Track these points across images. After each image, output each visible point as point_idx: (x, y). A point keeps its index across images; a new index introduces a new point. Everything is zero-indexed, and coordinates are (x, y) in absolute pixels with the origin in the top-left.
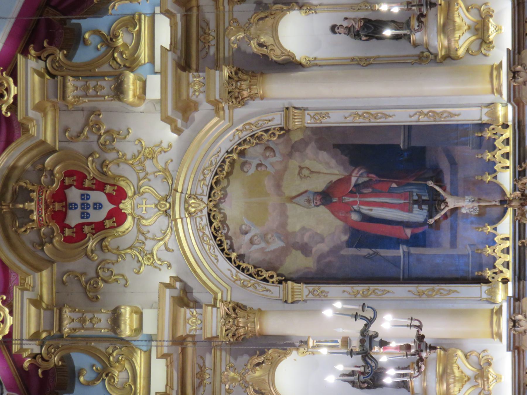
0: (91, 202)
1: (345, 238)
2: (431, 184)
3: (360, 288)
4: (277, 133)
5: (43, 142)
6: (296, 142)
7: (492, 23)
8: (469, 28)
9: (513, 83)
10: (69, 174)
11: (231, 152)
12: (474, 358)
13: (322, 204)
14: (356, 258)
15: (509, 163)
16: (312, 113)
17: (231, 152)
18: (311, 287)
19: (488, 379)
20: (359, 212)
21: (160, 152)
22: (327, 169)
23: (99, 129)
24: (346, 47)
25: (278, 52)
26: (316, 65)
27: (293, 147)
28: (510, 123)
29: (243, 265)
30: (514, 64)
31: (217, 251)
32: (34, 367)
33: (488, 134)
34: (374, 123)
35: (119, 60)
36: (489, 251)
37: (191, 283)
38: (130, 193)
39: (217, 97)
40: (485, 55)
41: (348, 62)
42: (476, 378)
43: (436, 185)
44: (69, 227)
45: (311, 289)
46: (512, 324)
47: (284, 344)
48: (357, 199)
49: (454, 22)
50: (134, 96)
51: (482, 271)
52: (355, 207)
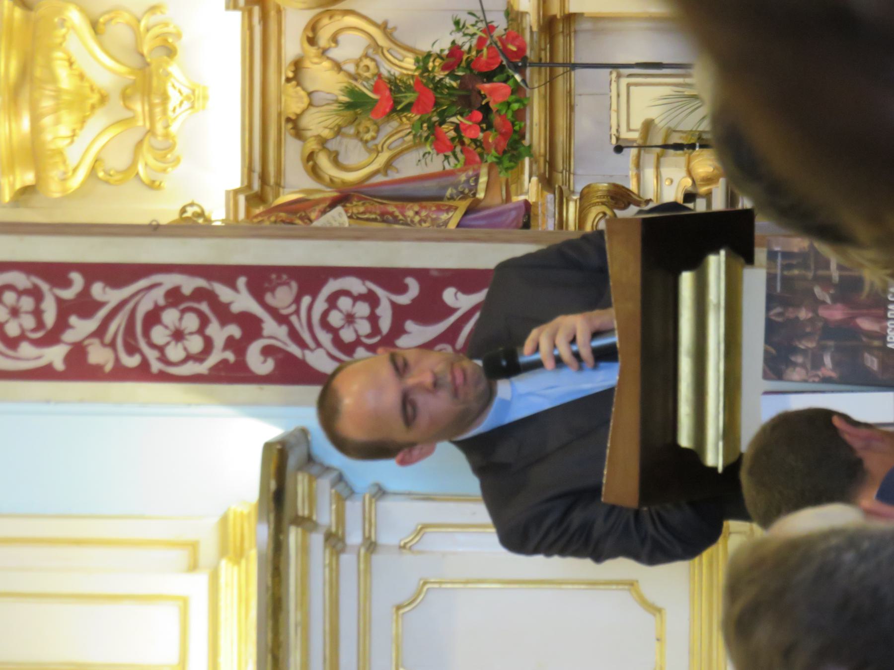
12: (119, 31)
19: (165, 98)
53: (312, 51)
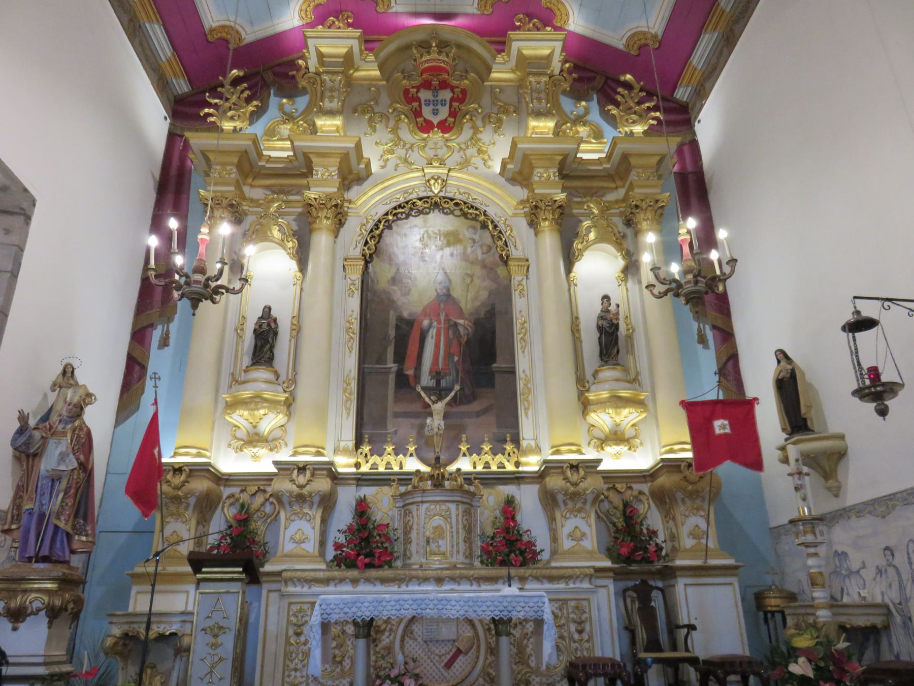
0: (439, 106)
1: (405, 314)
2: (457, 387)
3: (356, 326)
4: (504, 253)
5: (489, 70)
6: (496, 273)
7: (623, 449)
8: (618, 425)
9: (565, 465)
10: (464, 92)
11: (485, 215)
13: (438, 294)
14: (386, 323)
15: (480, 468)
16: (524, 282)
17: (485, 215)
18: (358, 283)
19: (254, 447)
20: (430, 326)
21: (483, 159)
22: (470, 298)
23: (503, 113)
24: (589, 311)
25: (580, 246)
26: (569, 286)
27: (491, 268)
28: (521, 469)
29: (381, 227)
30: (587, 467)
31: (393, 205)
32: (298, 68)
33: (509, 447)
34: (517, 337)
35: (564, 127)
36: (389, 449)
37: (366, 184)
38: (446, 135)
39: (536, 191)
40: (589, 444)
41: (575, 315)
42: (257, 434)
43: (456, 394)
44: (417, 92)
45: (357, 282)
46: (301, 466)
47: (302, 257)
48: (442, 325)
49: (625, 408)
50: (534, 128)
51: (370, 442)
52: (435, 324)
53: (268, 495)
